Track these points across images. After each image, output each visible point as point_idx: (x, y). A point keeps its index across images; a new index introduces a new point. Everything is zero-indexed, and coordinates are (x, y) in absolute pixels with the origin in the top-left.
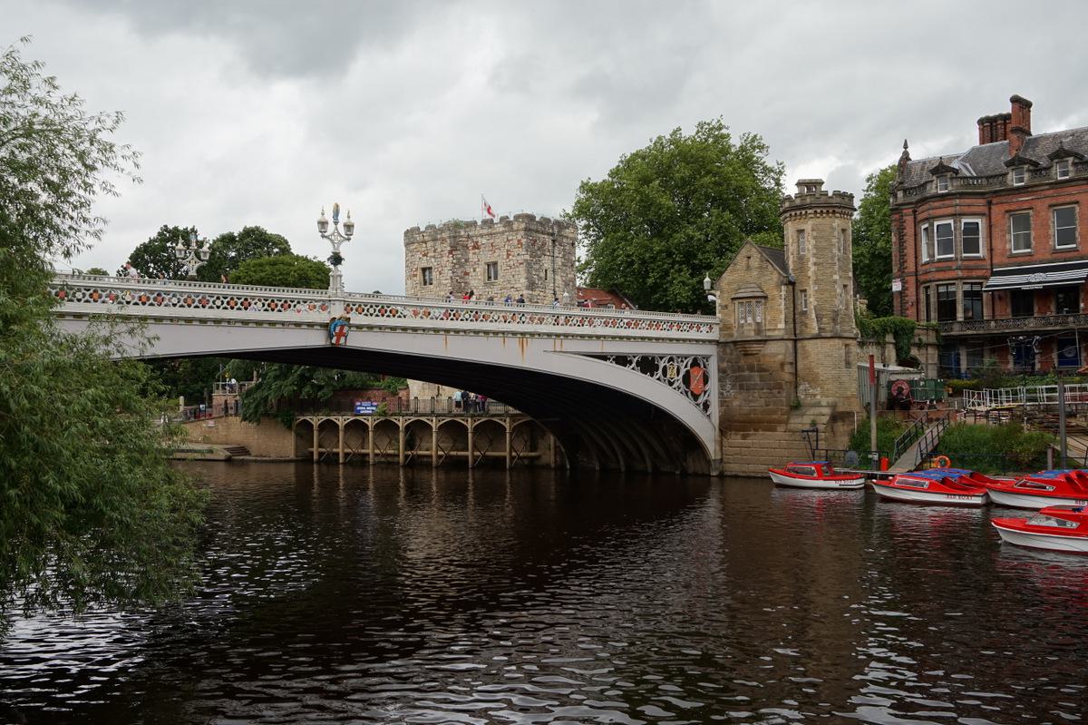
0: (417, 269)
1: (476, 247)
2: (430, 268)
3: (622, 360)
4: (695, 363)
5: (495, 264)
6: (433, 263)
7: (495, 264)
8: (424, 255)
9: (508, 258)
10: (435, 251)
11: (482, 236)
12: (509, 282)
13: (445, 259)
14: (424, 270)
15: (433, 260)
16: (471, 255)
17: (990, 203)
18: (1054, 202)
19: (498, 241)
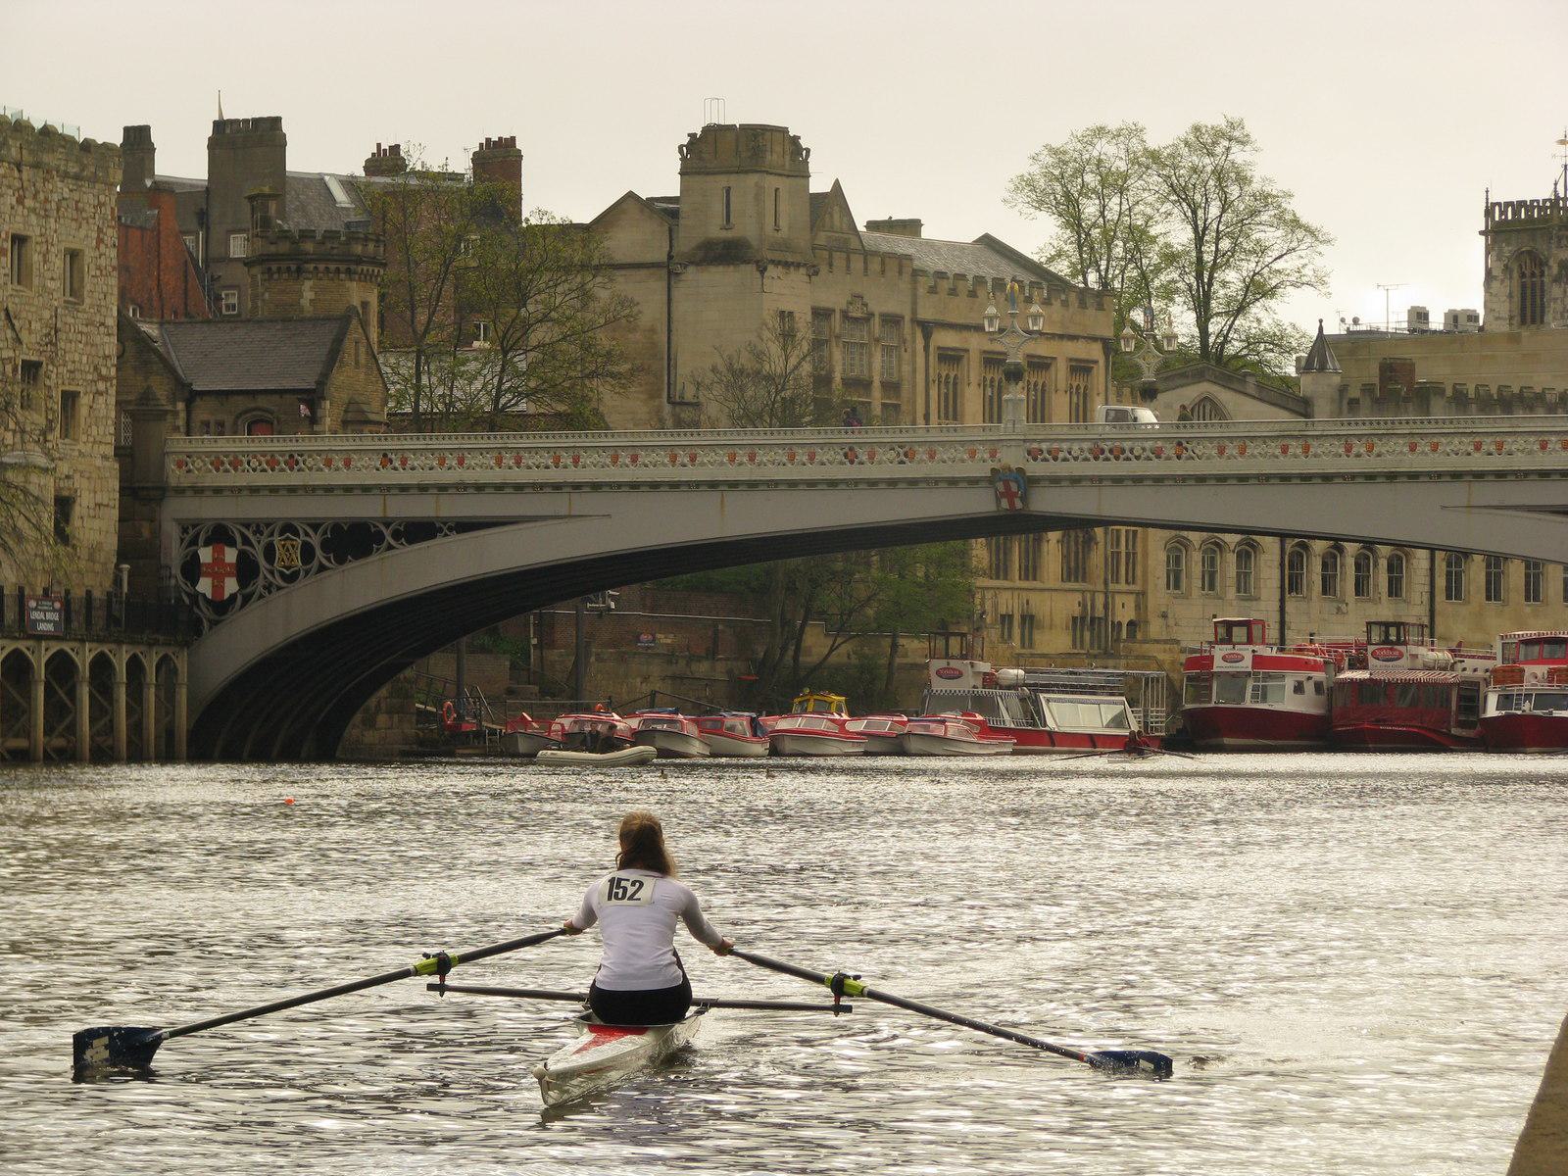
6: (33, 232)
9: (98, 247)
10: (35, 197)
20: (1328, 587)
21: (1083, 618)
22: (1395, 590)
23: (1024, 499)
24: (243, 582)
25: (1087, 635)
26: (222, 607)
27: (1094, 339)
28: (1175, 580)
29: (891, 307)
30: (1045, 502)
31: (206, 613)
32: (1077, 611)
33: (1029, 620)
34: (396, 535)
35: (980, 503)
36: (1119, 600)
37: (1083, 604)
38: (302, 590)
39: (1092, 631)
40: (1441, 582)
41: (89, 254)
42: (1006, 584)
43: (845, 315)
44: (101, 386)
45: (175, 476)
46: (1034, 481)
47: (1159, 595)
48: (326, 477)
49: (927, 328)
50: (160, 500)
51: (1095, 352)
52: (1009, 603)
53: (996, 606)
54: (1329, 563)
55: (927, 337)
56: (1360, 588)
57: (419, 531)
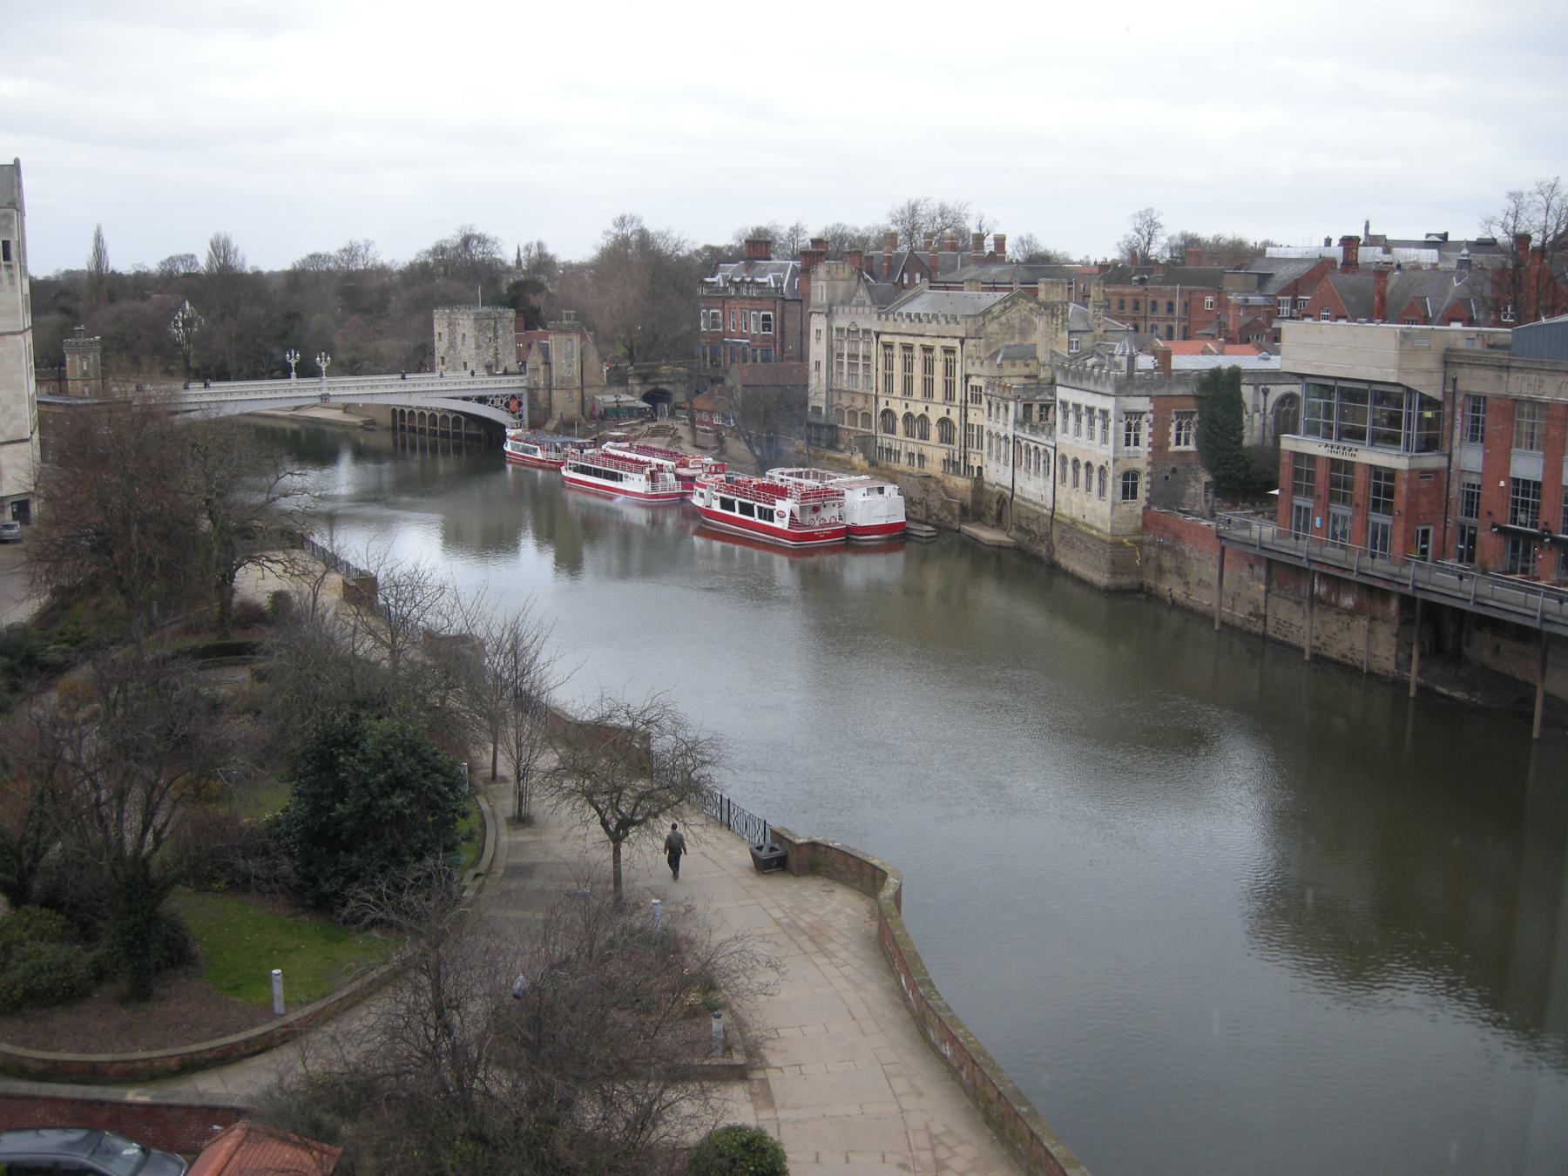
3: (466, 399)
4: (513, 397)
21: (949, 461)
25: (951, 469)
27: (956, 338)
29: (867, 326)
32: (946, 457)
33: (922, 457)
36: (972, 456)
37: (948, 454)
39: (953, 467)
42: (912, 440)
43: (848, 330)
49: (878, 335)
51: (956, 343)
52: (912, 448)
53: (906, 448)
55: (877, 338)
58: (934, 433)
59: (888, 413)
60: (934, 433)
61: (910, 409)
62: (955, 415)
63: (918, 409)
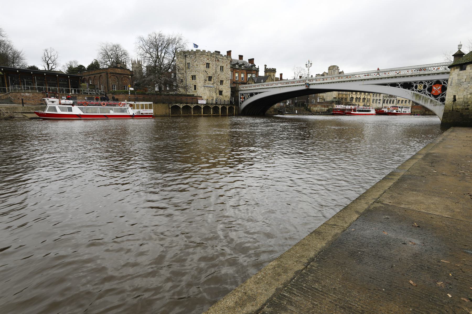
0: (205, 63)
1: (218, 61)
2: (209, 64)
5: (223, 67)
6: (210, 62)
7: (223, 67)
8: (208, 59)
11: (220, 58)
12: (227, 72)
13: (214, 62)
14: (207, 63)
15: (211, 62)
16: (217, 63)
17: (233, 70)
18: (242, 72)
19: (224, 61)
20: (387, 103)
22: (393, 103)
23: (309, 87)
24: (244, 99)
26: (243, 102)
28: (373, 102)
30: (312, 87)
31: (241, 102)
33: (359, 105)
34: (255, 94)
35: (304, 88)
38: (248, 100)
40: (397, 102)
41: (224, 67)
44: (227, 80)
45: (239, 89)
46: (310, 84)
47: (371, 103)
48: (246, 89)
50: (238, 92)
54: (390, 101)
56: (390, 103)
57: (256, 93)
58: (361, 100)
59: (352, 98)
60: (361, 100)
61: (357, 97)
62: (366, 97)
63: (358, 96)
